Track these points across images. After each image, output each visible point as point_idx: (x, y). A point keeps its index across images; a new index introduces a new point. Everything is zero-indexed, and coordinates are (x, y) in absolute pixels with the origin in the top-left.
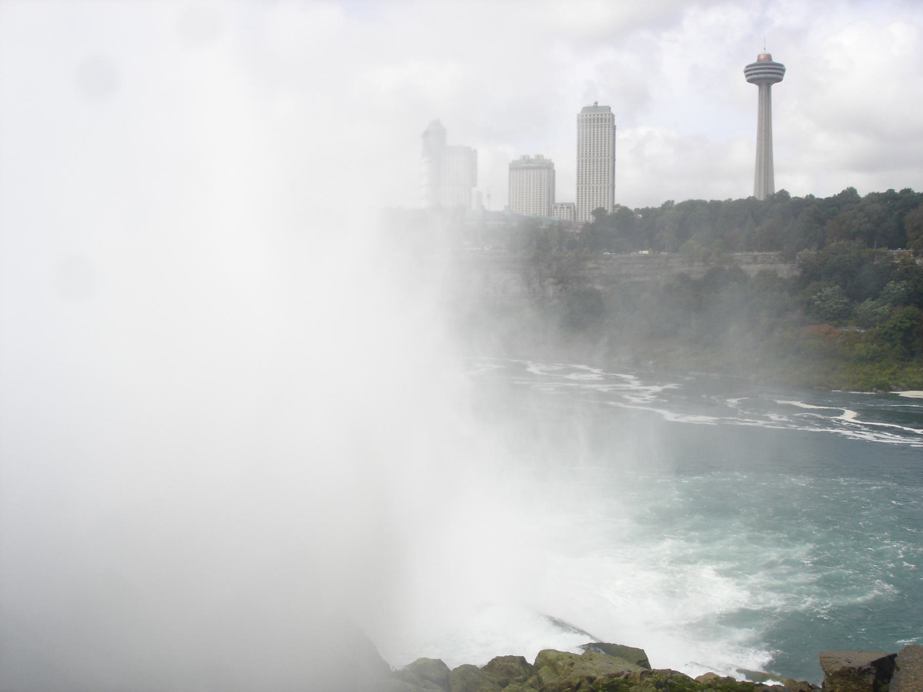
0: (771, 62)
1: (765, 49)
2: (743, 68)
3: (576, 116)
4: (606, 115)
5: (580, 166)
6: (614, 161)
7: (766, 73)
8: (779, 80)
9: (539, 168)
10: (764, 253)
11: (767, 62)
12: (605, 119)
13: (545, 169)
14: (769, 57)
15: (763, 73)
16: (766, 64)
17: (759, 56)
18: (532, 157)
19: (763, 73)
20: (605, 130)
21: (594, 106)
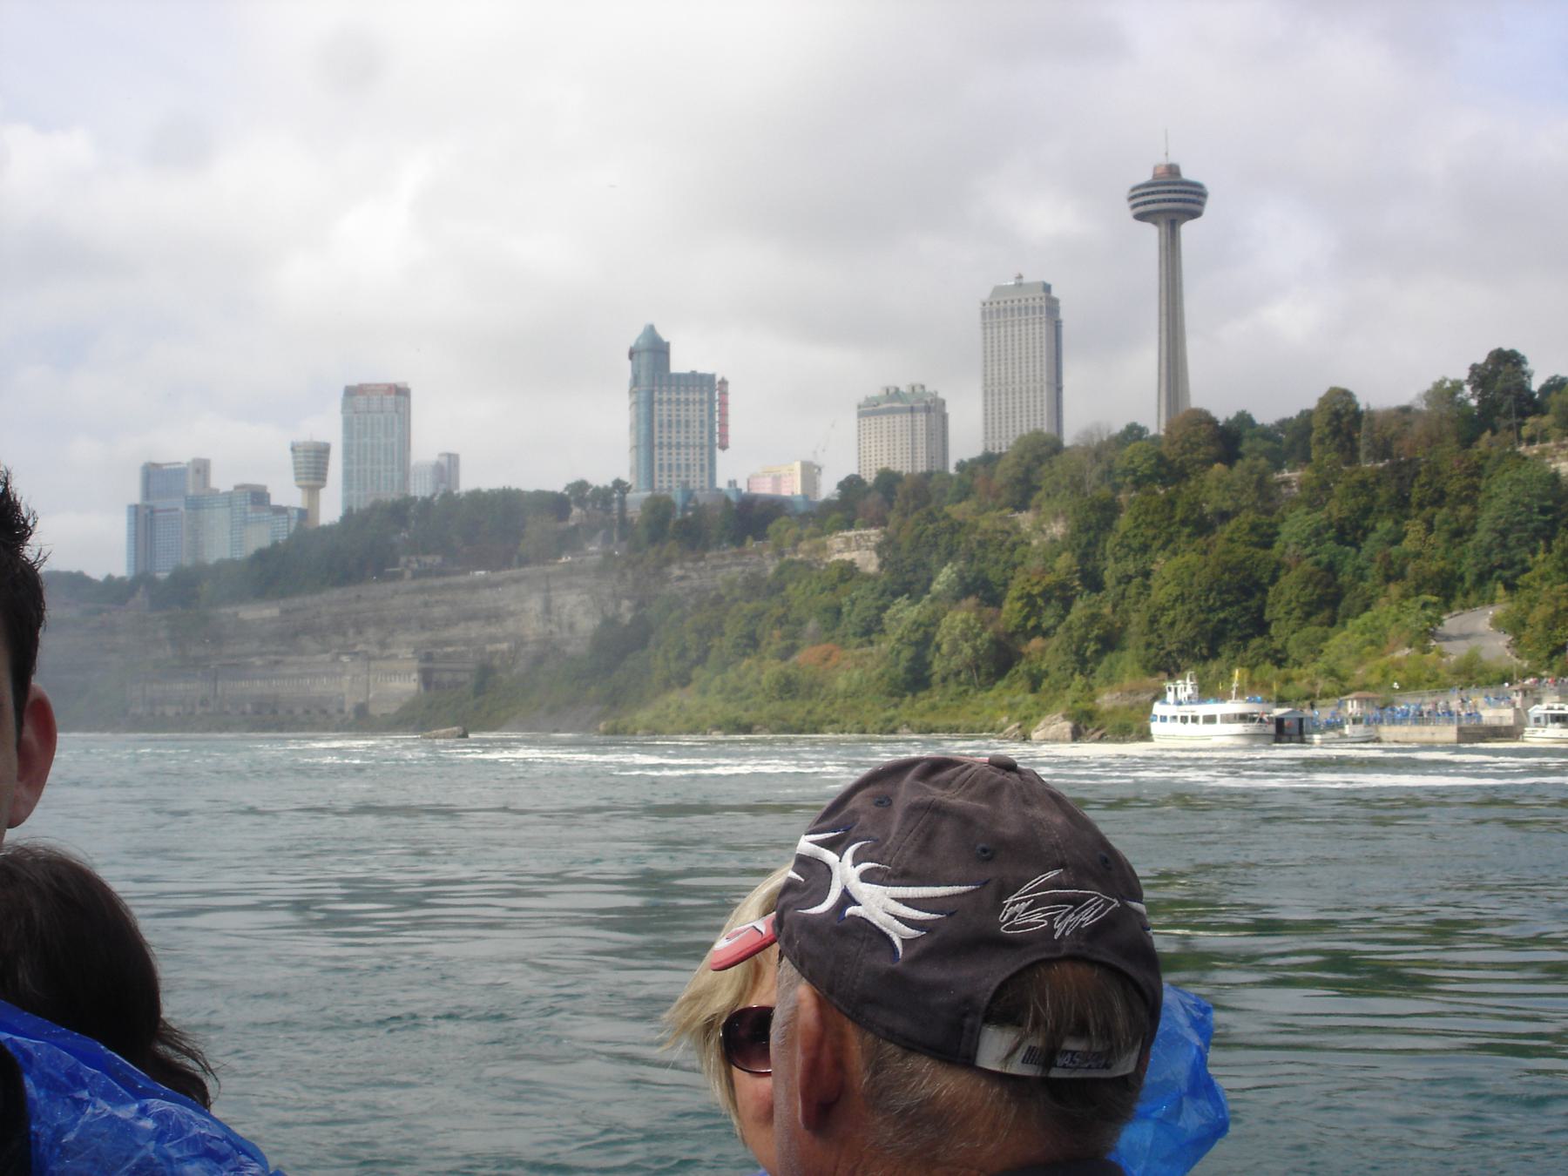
0: (1178, 180)
1: (1167, 154)
3: (980, 305)
4: (1034, 299)
5: (989, 403)
6: (1059, 390)
7: (1159, 201)
8: (1195, 214)
9: (912, 410)
10: (863, 532)
11: (1172, 180)
12: (1034, 308)
13: (934, 411)
14: (1173, 170)
15: (1154, 202)
16: (1168, 184)
17: (1155, 169)
18: (904, 389)
19: (1154, 202)
20: (1034, 329)
21: (1016, 285)
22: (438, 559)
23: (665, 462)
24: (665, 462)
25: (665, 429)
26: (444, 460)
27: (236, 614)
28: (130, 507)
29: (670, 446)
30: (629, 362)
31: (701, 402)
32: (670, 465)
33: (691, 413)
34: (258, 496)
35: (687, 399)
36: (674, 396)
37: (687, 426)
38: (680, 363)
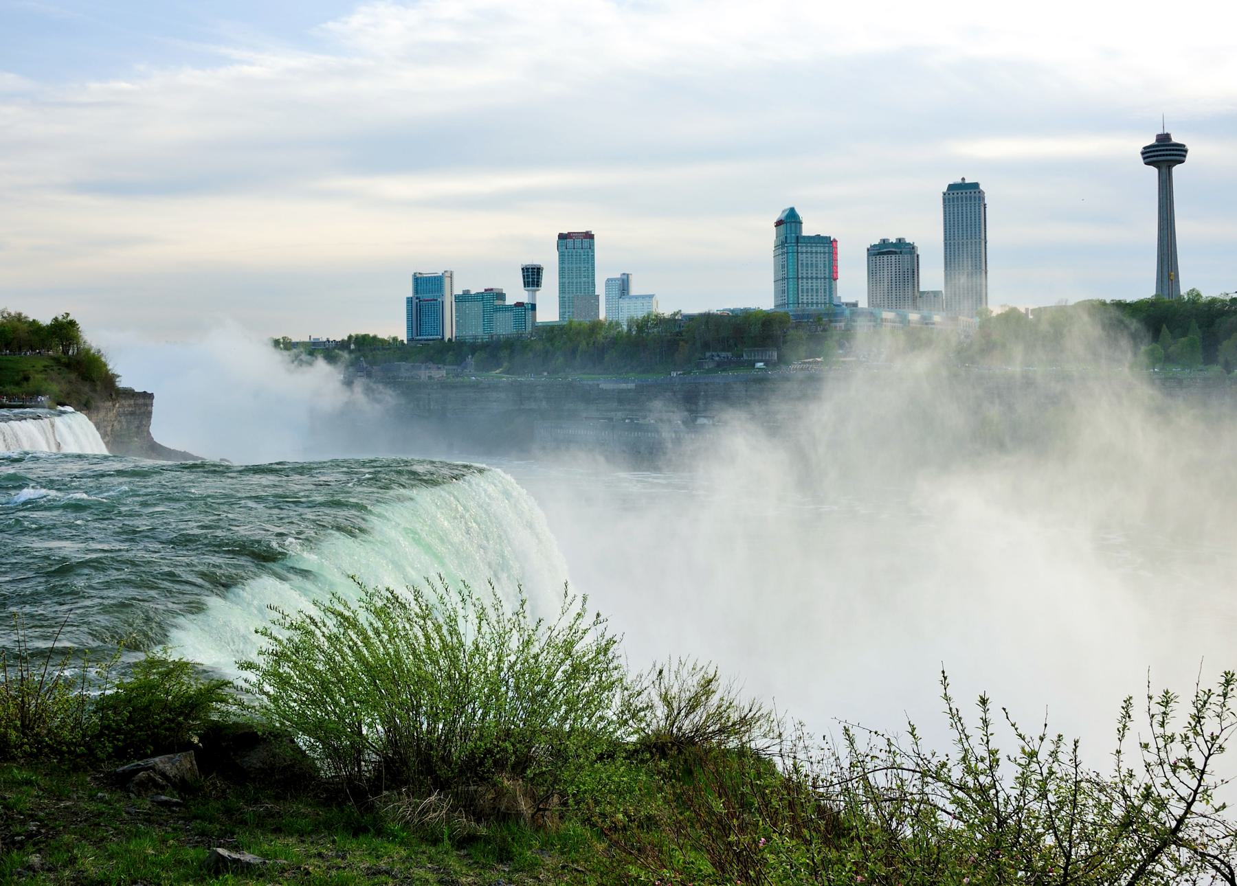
2: (1140, 149)
12: (975, 197)
22: (729, 354)
23: (805, 288)
24: (805, 288)
25: (805, 269)
26: (625, 277)
27: (598, 385)
28: (408, 298)
29: (807, 278)
30: (773, 230)
31: (825, 253)
32: (807, 289)
33: (819, 259)
34: (501, 296)
35: (816, 253)
36: (809, 249)
37: (817, 267)
38: (808, 230)
